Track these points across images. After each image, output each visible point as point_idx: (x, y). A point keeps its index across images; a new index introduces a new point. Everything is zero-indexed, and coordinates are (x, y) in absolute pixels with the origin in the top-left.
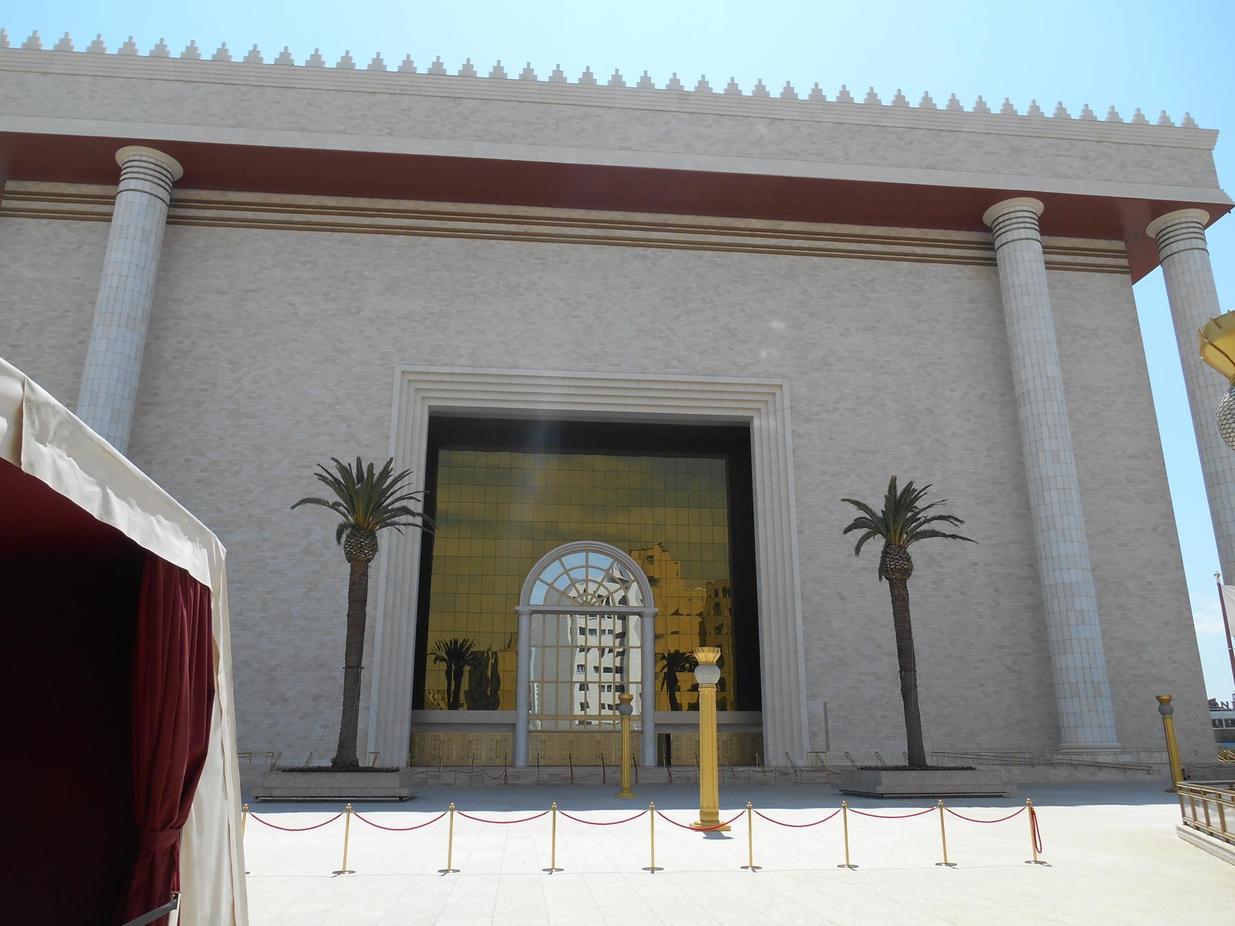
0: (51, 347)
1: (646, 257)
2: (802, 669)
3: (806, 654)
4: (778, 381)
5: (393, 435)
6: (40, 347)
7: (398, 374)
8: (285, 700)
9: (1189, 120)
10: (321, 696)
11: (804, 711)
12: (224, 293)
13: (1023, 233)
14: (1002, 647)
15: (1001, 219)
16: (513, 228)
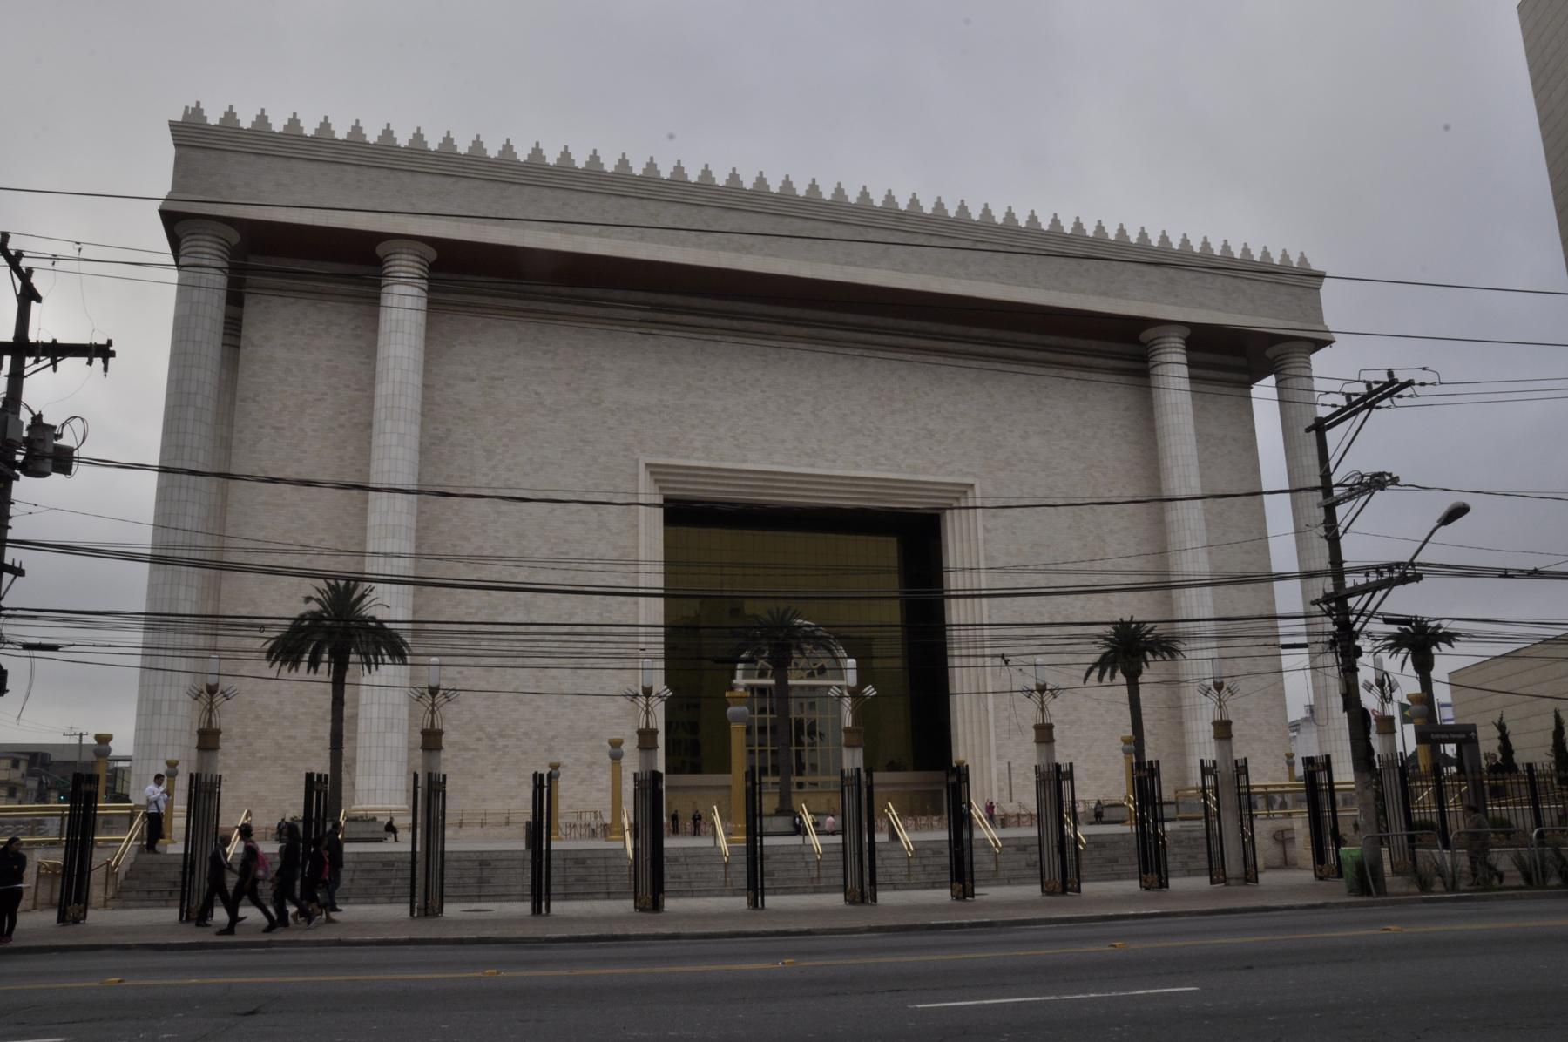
2: (992, 735)
3: (996, 720)
4: (969, 480)
5: (642, 526)
7: (642, 467)
9: (1303, 259)
11: (994, 770)
13: (1175, 358)
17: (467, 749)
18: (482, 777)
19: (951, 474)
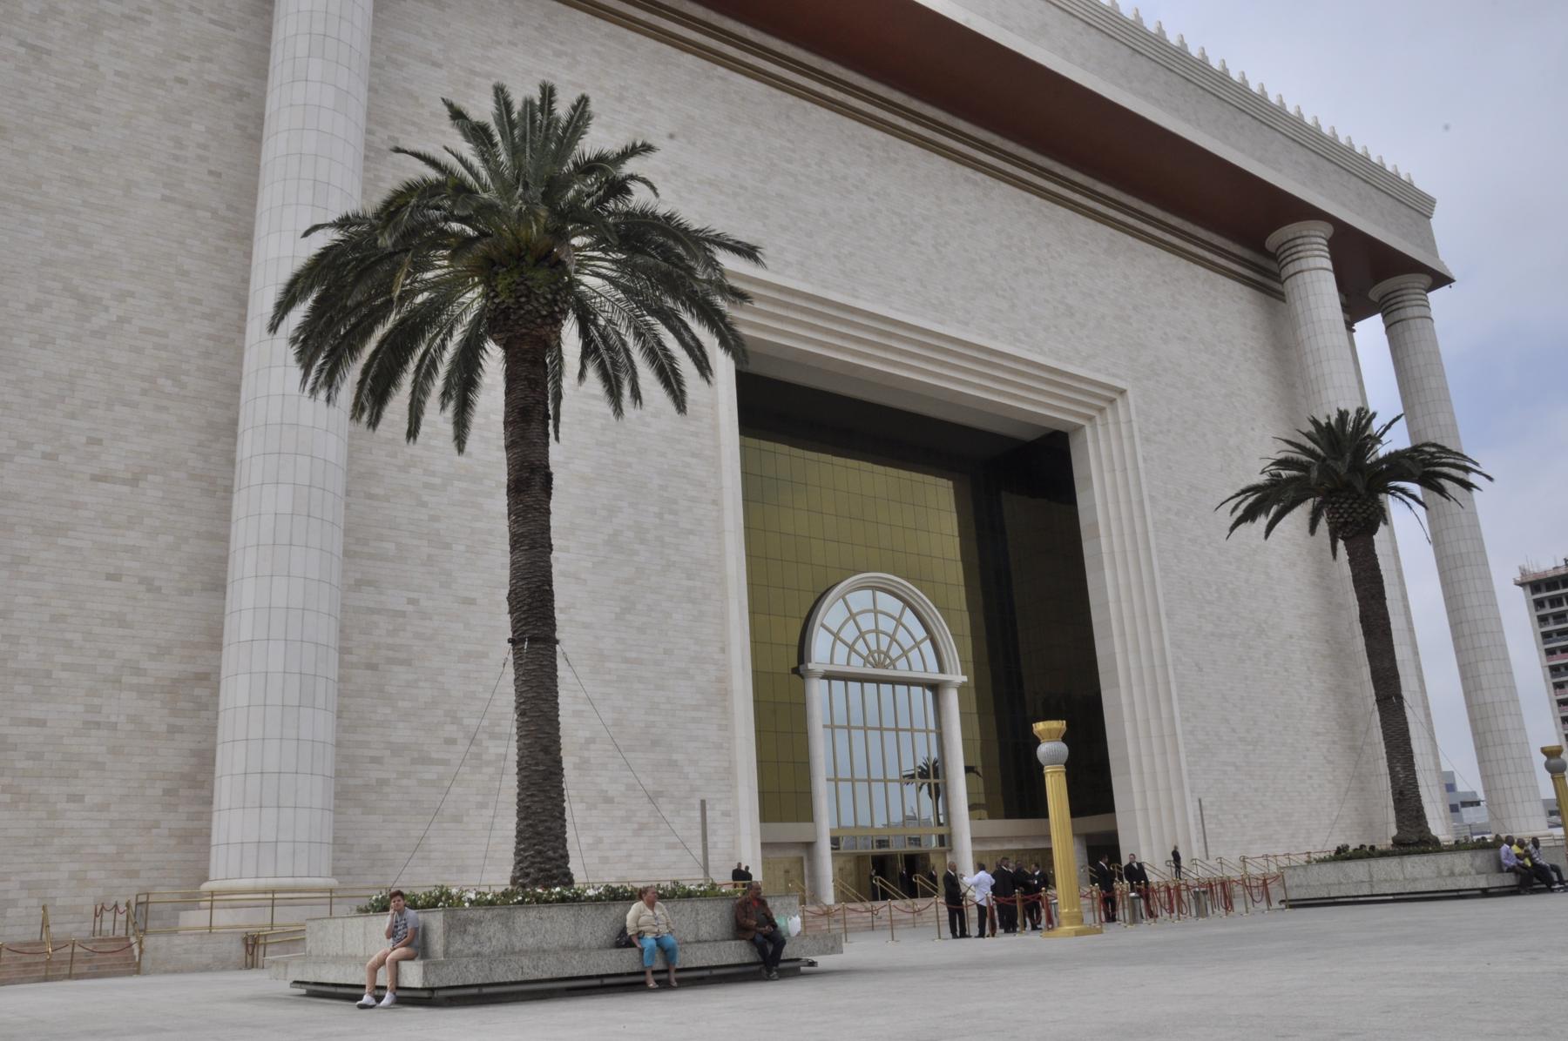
0: (117, 73)
1: (975, 183)
6: (95, 67)
8: (609, 800)
10: (659, 794)
12: (436, 64)
14: (1318, 734)
15: (1299, 241)
16: (828, 91)
17: (426, 760)
18: (457, 819)
19: (1099, 371)
